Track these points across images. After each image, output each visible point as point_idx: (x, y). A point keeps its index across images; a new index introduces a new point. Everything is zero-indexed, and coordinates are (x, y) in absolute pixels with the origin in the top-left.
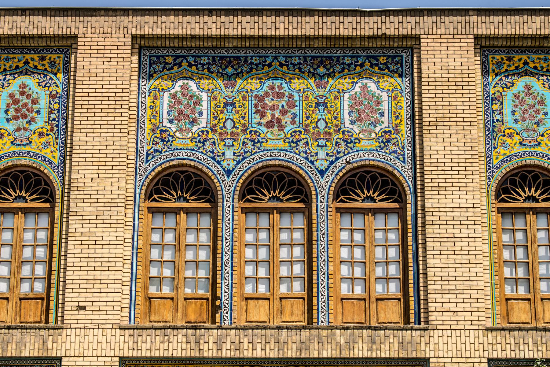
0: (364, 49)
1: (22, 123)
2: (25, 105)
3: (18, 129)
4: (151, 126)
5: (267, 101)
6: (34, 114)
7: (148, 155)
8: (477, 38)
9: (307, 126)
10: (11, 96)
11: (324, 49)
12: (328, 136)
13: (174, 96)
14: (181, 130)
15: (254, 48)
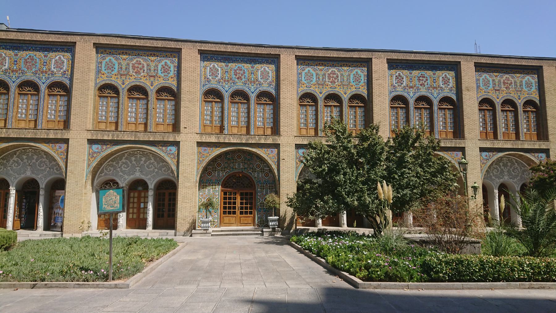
0: (264, 57)
1: (166, 74)
2: (167, 69)
3: (165, 76)
4: (204, 77)
5: (237, 71)
6: (169, 71)
7: (203, 85)
8: (296, 56)
9: (249, 79)
10: (162, 65)
11: (253, 57)
12: (254, 82)
13: (210, 68)
14: (213, 79)
15: (234, 55)
